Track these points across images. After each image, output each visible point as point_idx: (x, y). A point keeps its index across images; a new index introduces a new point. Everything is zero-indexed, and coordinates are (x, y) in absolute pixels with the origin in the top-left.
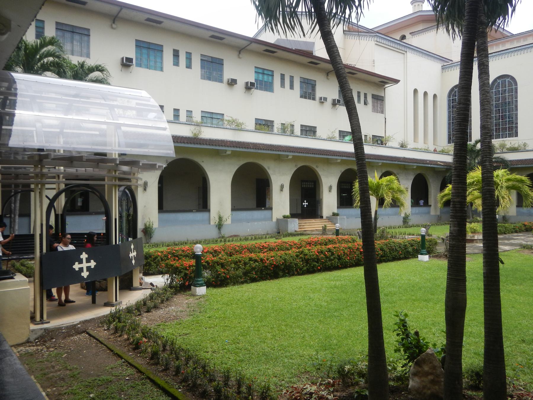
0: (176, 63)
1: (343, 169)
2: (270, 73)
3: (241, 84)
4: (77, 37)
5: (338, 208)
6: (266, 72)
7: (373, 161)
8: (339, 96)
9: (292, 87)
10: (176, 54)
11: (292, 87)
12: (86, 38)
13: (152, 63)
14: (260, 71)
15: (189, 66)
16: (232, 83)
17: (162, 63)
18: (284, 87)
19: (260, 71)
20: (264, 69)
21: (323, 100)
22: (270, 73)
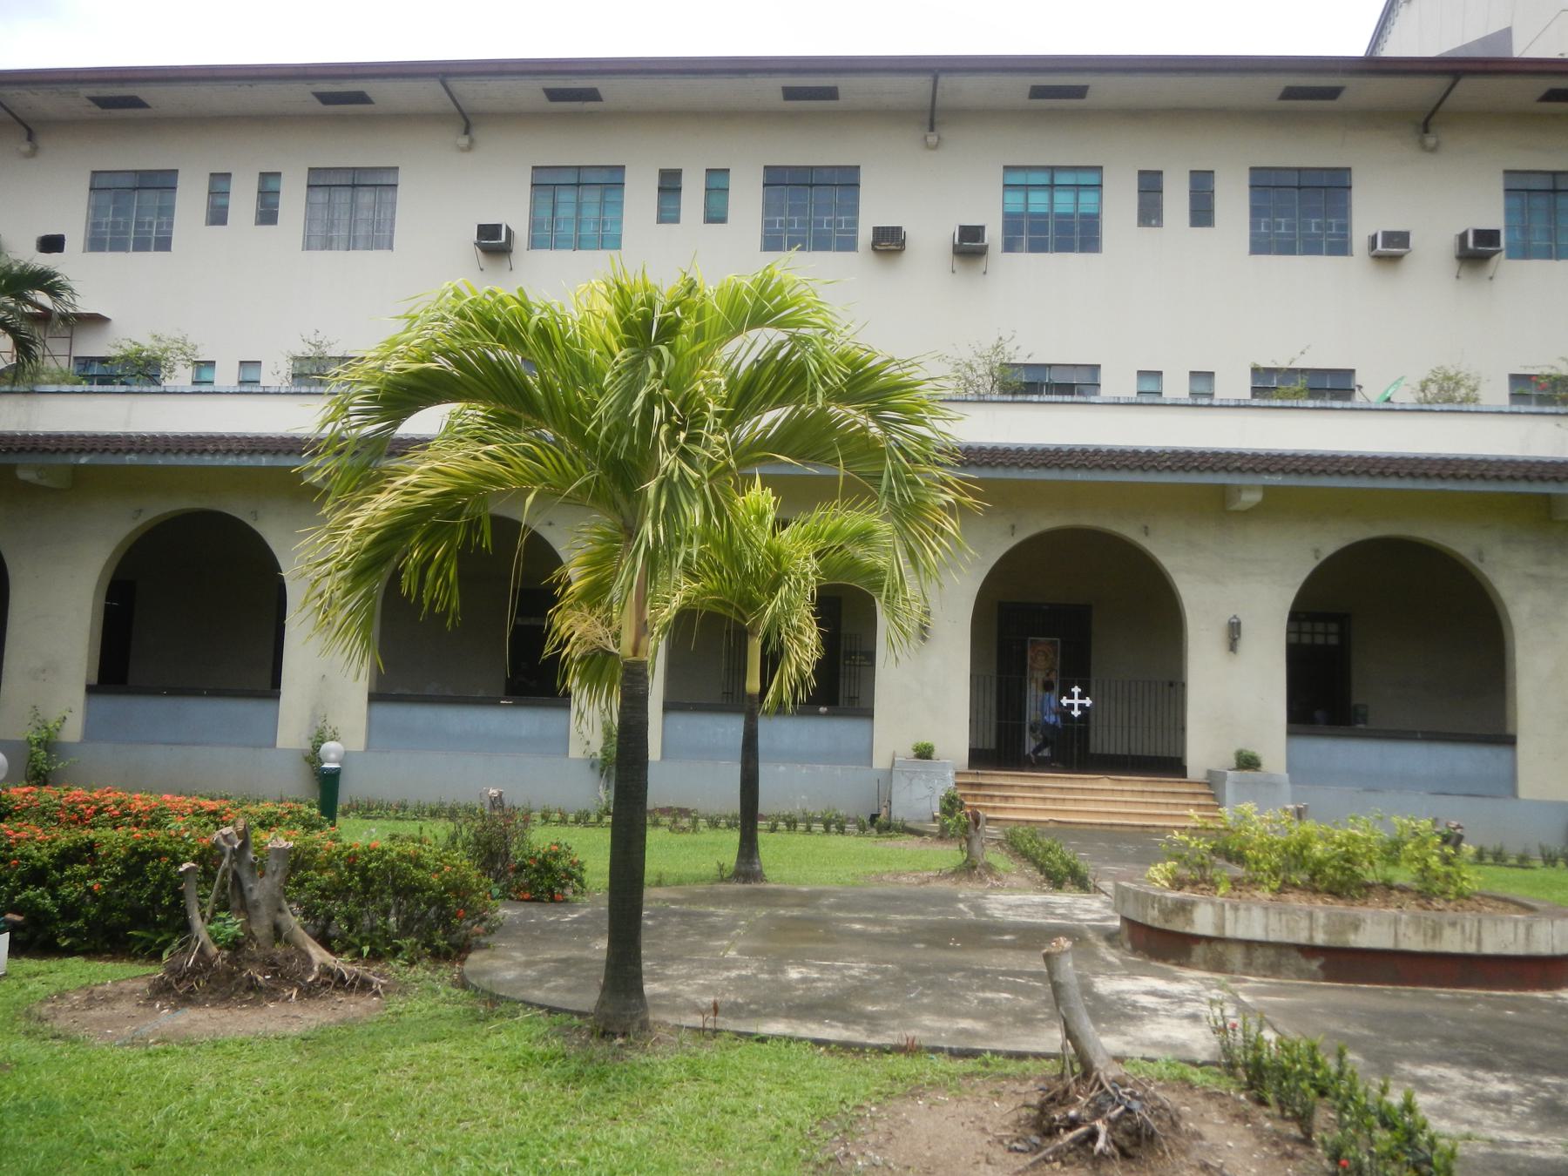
0: (668, 212)
1: (1331, 540)
2: (1090, 179)
3: (931, 236)
4: (366, 197)
5: (1290, 733)
6: (1061, 179)
7: (1550, 488)
8: (1509, 212)
9: (1202, 213)
10: (670, 184)
11: (1202, 213)
12: (387, 195)
13: (588, 230)
14: (1043, 179)
15: (715, 216)
16: (889, 242)
17: (619, 222)
18: (1160, 224)
19: (1043, 179)
20: (1052, 170)
21: (1392, 249)
22: (1090, 179)
